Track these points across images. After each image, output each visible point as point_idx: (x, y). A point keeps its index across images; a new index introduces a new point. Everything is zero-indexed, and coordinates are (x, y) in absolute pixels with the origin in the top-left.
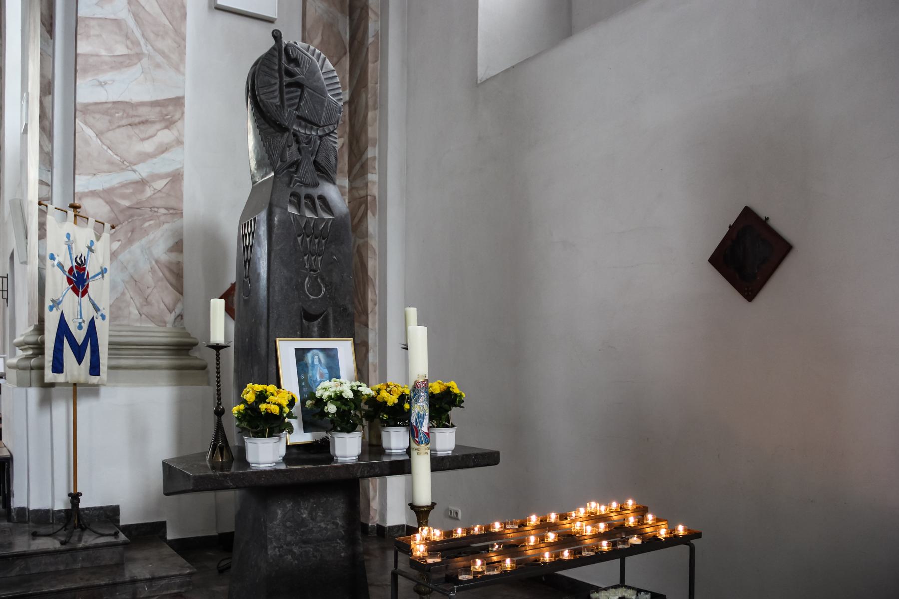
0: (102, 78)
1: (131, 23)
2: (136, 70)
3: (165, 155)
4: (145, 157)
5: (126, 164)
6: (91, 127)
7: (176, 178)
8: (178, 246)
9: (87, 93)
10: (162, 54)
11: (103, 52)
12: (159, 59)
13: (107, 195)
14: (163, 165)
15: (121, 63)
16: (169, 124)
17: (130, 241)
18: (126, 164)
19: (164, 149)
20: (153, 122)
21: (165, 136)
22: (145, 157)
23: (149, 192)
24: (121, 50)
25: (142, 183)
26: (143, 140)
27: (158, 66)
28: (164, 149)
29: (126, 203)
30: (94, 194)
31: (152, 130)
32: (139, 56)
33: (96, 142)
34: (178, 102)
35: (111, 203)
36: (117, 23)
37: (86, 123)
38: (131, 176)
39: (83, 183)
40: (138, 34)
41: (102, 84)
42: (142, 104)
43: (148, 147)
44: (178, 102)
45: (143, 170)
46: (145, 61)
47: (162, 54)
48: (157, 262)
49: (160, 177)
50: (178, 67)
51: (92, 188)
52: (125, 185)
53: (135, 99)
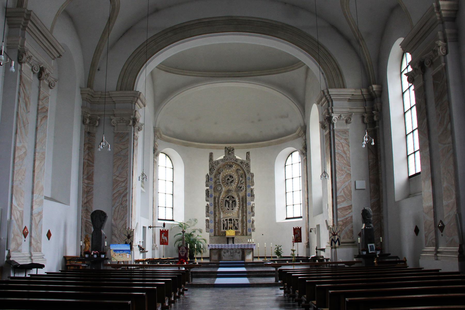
0: (341, 204)
1: (344, 195)
2: (345, 202)
3: (350, 214)
4: (347, 214)
5: (344, 216)
6: (340, 211)
7: (352, 217)
8: (352, 227)
9: (339, 207)
10: (348, 198)
11: (341, 200)
12: (348, 199)
13: (342, 221)
14: (349, 215)
15: (343, 201)
16: (350, 209)
17: (345, 227)
18: (344, 216)
19: (349, 213)
20: (348, 209)
21: (350, 211)
22: (347, 214)
23: (348, 220)
24: (343, 199)
25: (347, 218)
26: (347, 212)
27: (348, 201)
28: (349, 213)
29: (344, 222)
30: (340, 221)
31: (348, 210)
32: (345, 200)
33: (340, 213)
34: (351, 205)
35: (343, 222)
36: (342, 196)
37: (339, 211)
38: (345, 218)
39: (339, 220)
40: (345, 197)
41: (341, 205)
42: (346, 207)
43: (347, 213)
44: (351, 205)
45: (347, 216)
46: (346, 200)
47: (348, 198)
48: (349, 230)
49: (349, 217)
50: (351, 200)
51: (340, 220)
52: (344, 219)
53: (345, 206)
